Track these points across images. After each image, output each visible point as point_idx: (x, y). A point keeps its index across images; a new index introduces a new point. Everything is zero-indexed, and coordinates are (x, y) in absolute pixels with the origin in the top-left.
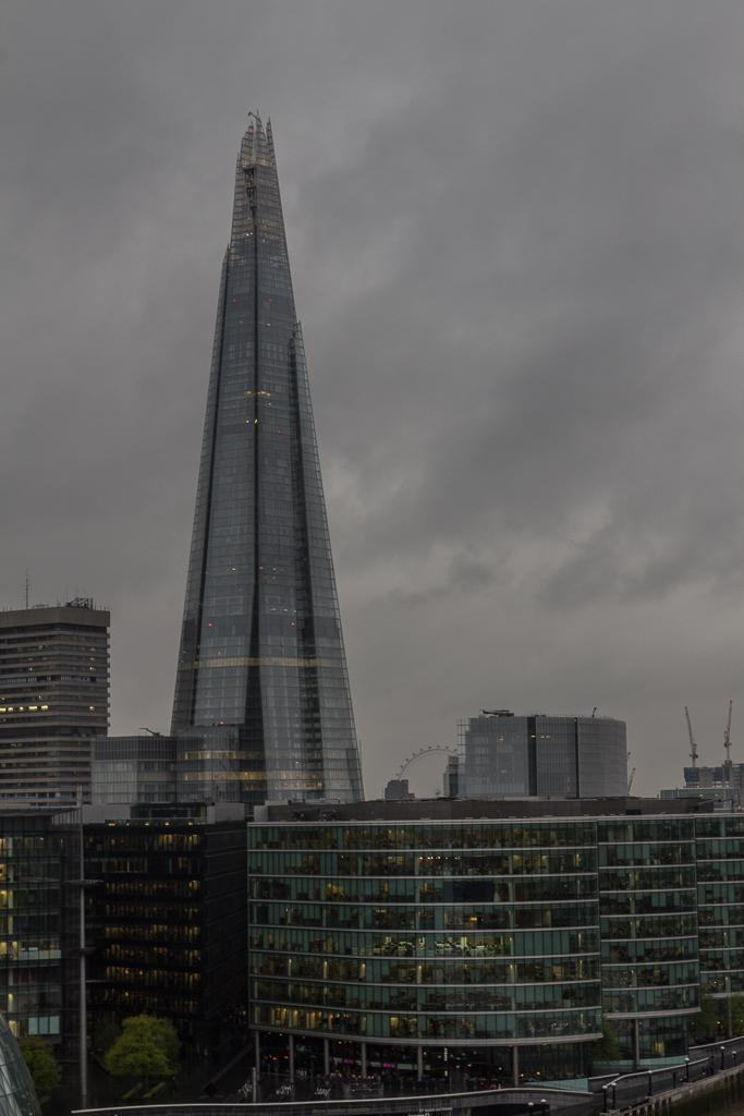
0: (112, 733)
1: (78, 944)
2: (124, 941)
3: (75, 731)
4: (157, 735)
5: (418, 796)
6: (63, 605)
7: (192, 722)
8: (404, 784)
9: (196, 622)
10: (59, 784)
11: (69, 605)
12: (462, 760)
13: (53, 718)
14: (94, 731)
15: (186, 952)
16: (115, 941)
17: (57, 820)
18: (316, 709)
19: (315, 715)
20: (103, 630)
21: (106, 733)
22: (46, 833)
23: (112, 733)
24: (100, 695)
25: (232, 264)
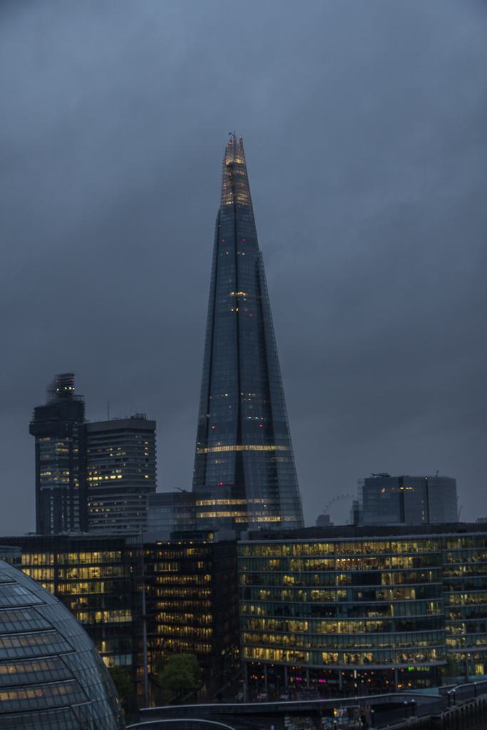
0: (158, 491)
1: (142, 612)
2: (169, 610)
3: (137, 490)
4: (184, 491)
5: (336, 524)
6: (129, 417)
7: (204, 484)
8: (327, 517)
9: (205, 427)
10: (129, 521)
11: (132, 418)
12: (361, 503)
13: (124, 483)
14: (148, 490)
15: (204, 616)
16: (163, 610)
17: (128, 541)
18: (276, 475)
19: (275, 478)
20: (152, 431)
21: (155, 491)
22: (123, 549)
23: (158, 491)
24: (152, 471)
25: (221, 220)
